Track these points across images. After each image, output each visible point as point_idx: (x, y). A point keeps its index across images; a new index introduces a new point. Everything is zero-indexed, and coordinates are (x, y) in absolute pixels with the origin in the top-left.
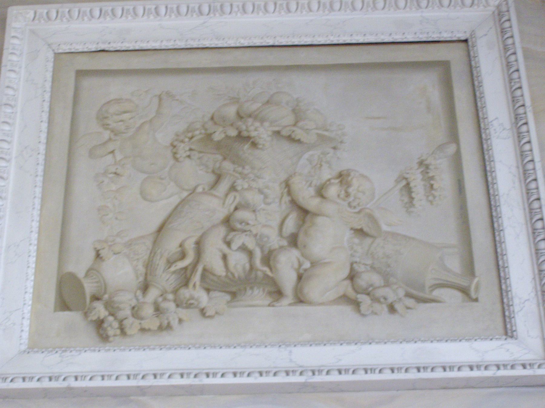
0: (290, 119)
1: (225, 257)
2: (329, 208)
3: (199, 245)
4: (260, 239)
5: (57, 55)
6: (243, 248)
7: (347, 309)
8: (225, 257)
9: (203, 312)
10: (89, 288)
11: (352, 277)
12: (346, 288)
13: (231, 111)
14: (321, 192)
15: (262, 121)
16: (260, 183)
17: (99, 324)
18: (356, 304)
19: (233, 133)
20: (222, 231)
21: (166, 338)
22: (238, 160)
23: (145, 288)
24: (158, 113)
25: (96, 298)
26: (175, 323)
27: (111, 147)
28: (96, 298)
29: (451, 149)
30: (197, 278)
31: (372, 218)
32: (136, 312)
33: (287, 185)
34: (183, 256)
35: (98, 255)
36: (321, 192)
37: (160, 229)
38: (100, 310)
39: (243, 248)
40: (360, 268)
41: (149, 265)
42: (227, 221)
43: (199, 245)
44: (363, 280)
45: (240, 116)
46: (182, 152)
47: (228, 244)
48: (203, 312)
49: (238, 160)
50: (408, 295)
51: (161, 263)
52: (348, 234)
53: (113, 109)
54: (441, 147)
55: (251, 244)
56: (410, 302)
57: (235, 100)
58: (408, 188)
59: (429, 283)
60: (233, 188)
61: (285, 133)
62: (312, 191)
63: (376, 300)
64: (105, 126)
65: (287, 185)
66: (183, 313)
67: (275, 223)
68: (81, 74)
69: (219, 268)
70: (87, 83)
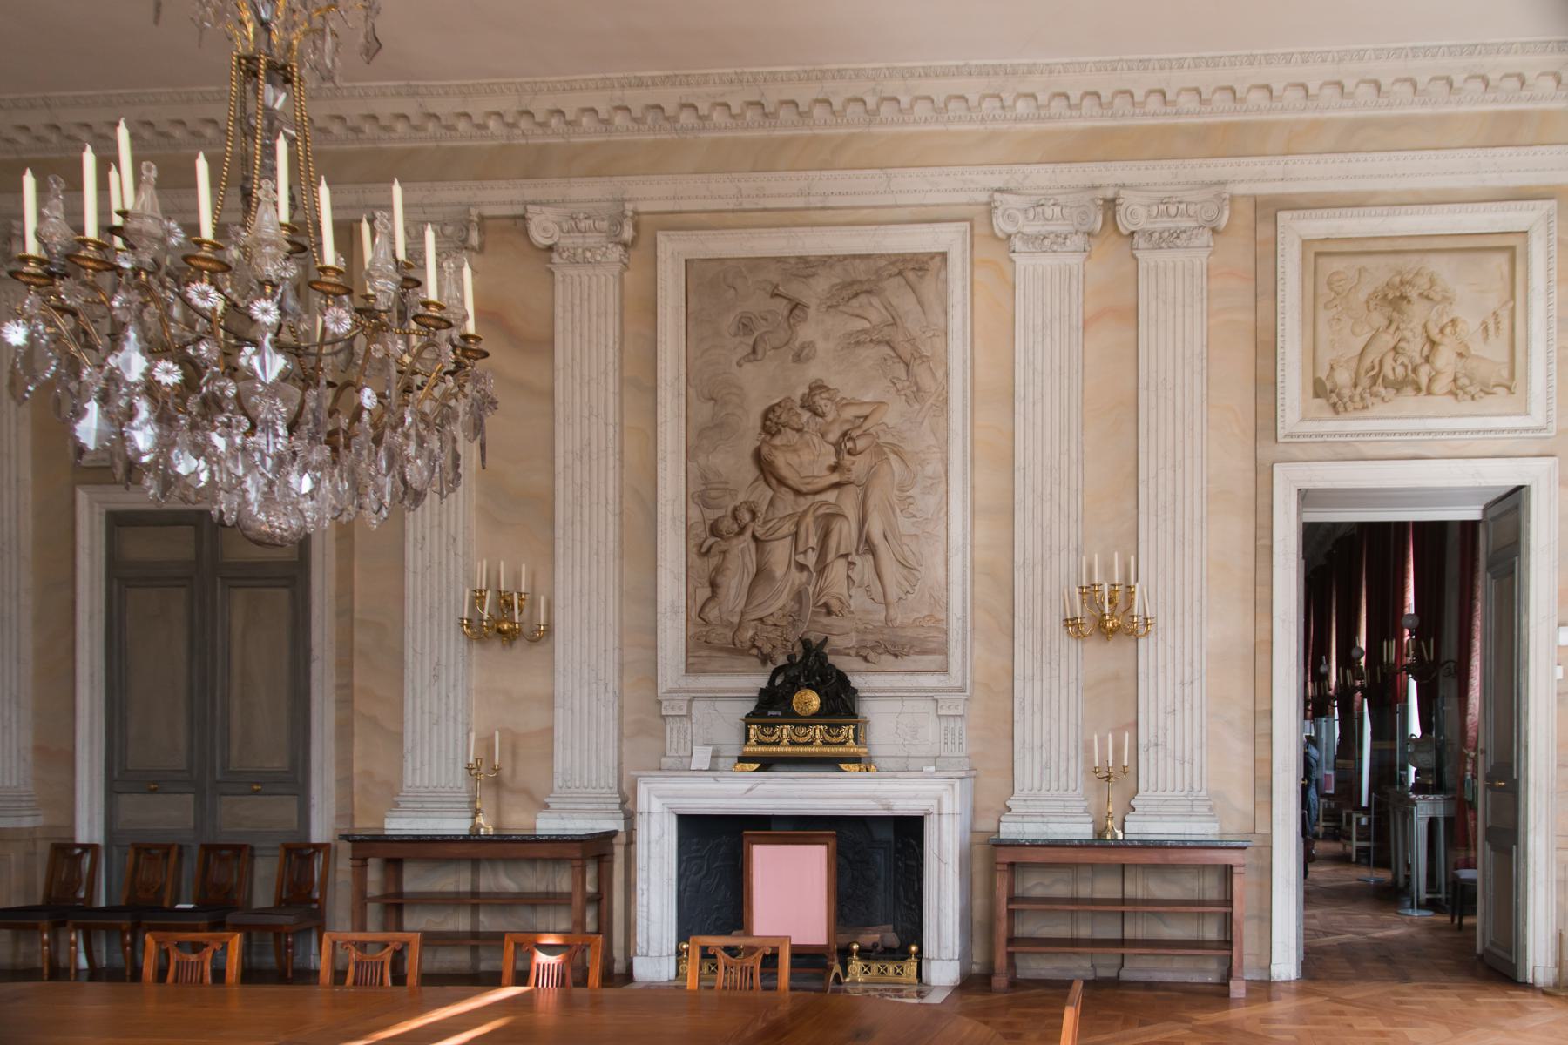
0: (1427, 286)
1: (1394, 369)
2: (1446, 340)
3: (1381, 361)
4: (1411, 359)
5: (1304, 242)
6: (1402, 364)
7: (1451, 398)
8: (1394, 369)
9: (1383, 399)
10: (1329, 386)
11: (1455, 380)
12: (1451, 386)
13: (1397, 280)
14: (1442, 331)
15: (1413, 286)
16: (1411, 326)
17: (1334, 405)
18: (1456, 395)
19: (1398, 294)
20: (1392, 354)
21: (1366, 413)
22: (1400, 312)
23: (1355, 386)
24: (1359, 280)
25: (1332, 391)
26: (1370, 405)
27: (1335, 303)
28: (1332, 391)
29: (1511, 304)
30: (1380, 380)
31: (1467, 347)
32: (1351, 399)
33: (1425, 326)
34: (1373, 368)
35: (1332, 368)
36: (1442, 331)
37: (1362, 352)
38: (1334, 398)
39: (1402, 364)
40: (1459, 375)
41: (1357, 374)
42: (1395, 348)
43: (1381, 361)
44: (1460, 383)
45: (1402, 283)
46: (1372, 306)
47: (1395, 361)
48: (1383, 399)
49: (1400, 312)
50: (1481, 390)
51: (1362, 372)
52: (1455, 355)
53: (1336, 278)
54: (1505, 303)
55: (1406, 362)
56: (1482, 394)
57: (1399, 273)
58: (1486, 329)
59: (1492, 383)
60: (1398, 328)
61: (1425, 294)
62: (1437, 330)
63: (1466, 393)
64: (1332, 289)
65: (1425, 326)
66: (1374, 400)
67: (1418, 349)
68: (1318, 254)
69: (1391, 376)
70: (1321, 260)
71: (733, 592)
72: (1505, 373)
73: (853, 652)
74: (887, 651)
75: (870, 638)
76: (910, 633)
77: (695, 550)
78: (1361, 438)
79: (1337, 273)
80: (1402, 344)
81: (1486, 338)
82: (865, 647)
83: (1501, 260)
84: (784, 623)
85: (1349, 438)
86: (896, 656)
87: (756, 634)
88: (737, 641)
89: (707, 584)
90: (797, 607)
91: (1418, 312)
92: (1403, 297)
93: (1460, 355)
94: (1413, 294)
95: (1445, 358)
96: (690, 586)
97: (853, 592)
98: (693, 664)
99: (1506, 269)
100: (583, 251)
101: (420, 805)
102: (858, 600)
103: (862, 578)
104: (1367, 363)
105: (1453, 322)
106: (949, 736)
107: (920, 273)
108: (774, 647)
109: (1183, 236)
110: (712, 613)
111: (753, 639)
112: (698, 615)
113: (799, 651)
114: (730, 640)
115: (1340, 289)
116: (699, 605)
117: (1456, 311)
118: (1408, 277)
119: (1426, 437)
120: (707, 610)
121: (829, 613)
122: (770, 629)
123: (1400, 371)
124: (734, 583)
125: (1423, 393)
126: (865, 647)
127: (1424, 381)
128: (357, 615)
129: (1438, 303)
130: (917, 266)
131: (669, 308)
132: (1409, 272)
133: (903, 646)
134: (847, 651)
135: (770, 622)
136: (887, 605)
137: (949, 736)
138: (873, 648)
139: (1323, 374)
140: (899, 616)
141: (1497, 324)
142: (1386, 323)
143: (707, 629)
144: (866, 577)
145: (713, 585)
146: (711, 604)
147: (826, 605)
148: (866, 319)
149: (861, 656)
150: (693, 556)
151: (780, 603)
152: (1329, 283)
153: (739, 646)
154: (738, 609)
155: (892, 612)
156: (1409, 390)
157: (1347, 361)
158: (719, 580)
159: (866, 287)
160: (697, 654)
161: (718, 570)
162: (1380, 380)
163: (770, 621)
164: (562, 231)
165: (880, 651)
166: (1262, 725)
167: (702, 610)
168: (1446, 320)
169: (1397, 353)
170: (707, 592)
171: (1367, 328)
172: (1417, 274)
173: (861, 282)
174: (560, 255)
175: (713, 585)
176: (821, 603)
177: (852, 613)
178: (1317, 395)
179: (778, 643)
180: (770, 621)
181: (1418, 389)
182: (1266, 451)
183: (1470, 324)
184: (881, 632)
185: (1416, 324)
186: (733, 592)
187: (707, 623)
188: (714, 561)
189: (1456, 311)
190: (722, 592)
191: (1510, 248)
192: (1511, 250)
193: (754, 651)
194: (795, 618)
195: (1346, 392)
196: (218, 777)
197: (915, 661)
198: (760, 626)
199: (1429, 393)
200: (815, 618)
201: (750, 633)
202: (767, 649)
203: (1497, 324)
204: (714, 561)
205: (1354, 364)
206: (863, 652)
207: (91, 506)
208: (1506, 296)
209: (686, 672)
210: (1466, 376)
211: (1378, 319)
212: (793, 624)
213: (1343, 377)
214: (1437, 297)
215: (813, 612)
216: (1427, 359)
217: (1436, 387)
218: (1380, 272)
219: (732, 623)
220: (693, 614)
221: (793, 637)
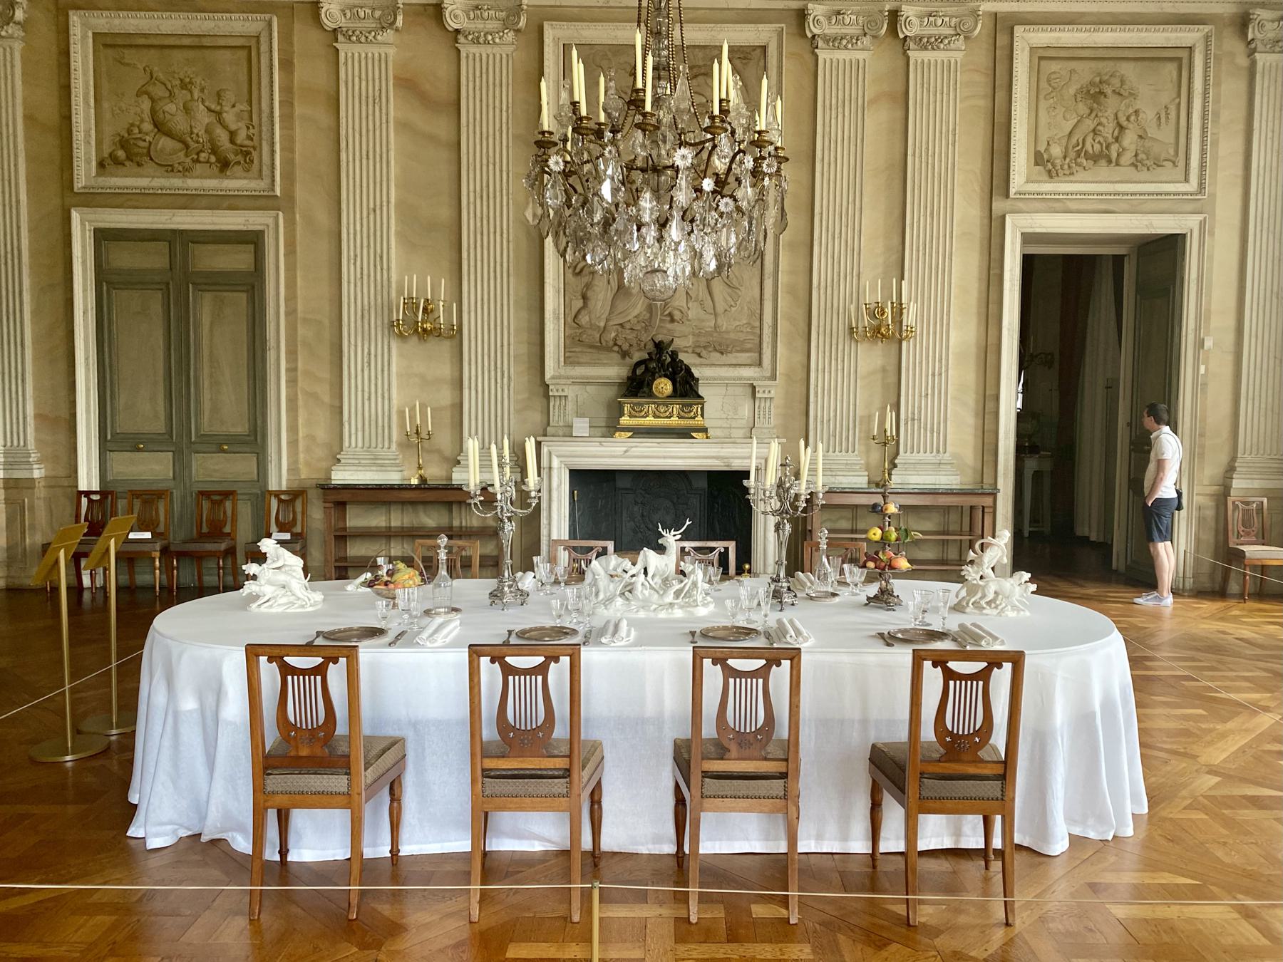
0: (1119, 85)
1: (1093, 146)
2: (1131, 126)
3: (1084, 141)
4: (1105, 139)
6: (1099, 142)
7: (1133, 168)
8: (1093, 146)
9: (1084, 168)
10: (1046, 157)
11: (1136, 155)
12: (1133, 160)
13: (1097, 79)
14: (1128, 119)
15: (1109, 85)
16: (1106, 114)
17: (1049, 171)
19: (1098, 90)
20: (1092, 134)
21: (1072, 178)
22: (1099, 104)
23: (1065, 158)
25: (1048, 161)
26: (1075, 172)
27: (1052, 95)
28: (1048, 161)
29: (1177, 101)
30: (1083, 154)
31: (1145, 130)
32: (1062, 168)
33: (1116, 115)
34: (1078, 145)
36: (1128, 119)
37: (1070, 133)
38: (1050, 166)
39: (1099, 142)
40: (1139, 152)
41: (1066, 148)
42: (1094, 131)
43: (1084, 141)
44: (1139, 158)
45: (1100, 82)
46: (1079, 99)
47: (1094, 140)
48: (1084, 168)
49: (1099, 104)
50: (1155, 164)
51: (1071, 148)
52: (1136, 137)
53: (1053, 76)
54: (1174, 100)
55: (1102, 140)
56: (1155, 166)
57: (1099, 74)
59: (1162, 158)
60: (1096, 116)
61: (1117, 91)
62: (1125, 118)
63: (1143, 165)
64: (1050, 85)
65: (1116, 115)
66: (1078, 168)
67: (1111, 132)
68: (1041, 58)
69: (1091, 152)
70: (1043, 63)
71: (600, 304)
72: (1172, 152)
73: (690, 350)
74: (716, 350)
75: (703, 340)
76: (732, 336)
77: (571, 270)
78: (1070, 197)
79: (1054, 73)
80: (1100, 128)
81: (1159, 125)
82: (699, 346)
83: (1171, 68)
84: (639, 328)
85: (1061, 197)
86: (722, 353)
87: (617, 335)
88: (603, 341)
89: (580, 297)
90: (648, 315)
91: (1112, 103)
92: (1101, 92)
93: (1140, 137)
94: (1108, 90)
95: (1129, 139)
96: (566, 298)
97: (690, 305)
98: (569, 357)
99: (1175, 74)
100: (485, 36)
101: (357, 462)
102: (694, 312)
103: (698, 295)
104: (1074, 141)
105: (1136, 112)
106: (762, 413)
107: (744, 61)
108: (631, 345)
109: (946, 41)
110: (584, 319)
111: (615, 339)
112: (573, 320)
113: (651, 347)
114: (598, 339)
115: (1056, 85)
116: (573, 314)
117: (1138, 105)
118: (1105, 78)
119: (1117, 197)
120: (580, 317)
121: (672, 320)
122: (628, 332)
123: (1097, 147)
124: (601, 296)
125: (1114, 164)
126: (699, 346)
127: (1114, 155)
128: (300, 315)
129: (1126, 98)
130: (742, 56)
131: (551, 82)
132: (1106, 74)
133: (728, 346)
134: (685, 349)
135: (628, 327)
136: (716, 315)
137: (762, 413)
138: (705, 347)
139: (1042, 148)
140: (724, 324)
141: (1167, 114)
142: (1088, 111)
143: (580, 331)
144: (701, 294)
145: (585, 297)
146: (583, 312)
147: (670, 315)
148: (703, 95)
149: (696, 353)
150: (569, 275)
151: (636, 312)
152: (1049, 81)
153: (604, 344)
154: (604, 316)
155: (719, 321)
156: (1103, 162)
157: (1059, 139)
158: (589, 294)
159: (703, 71)
160: (573, 350)
161: (588, 286)
162: (1083, 154)
163: (628, 326)
164: (469, 19)
165: (710, 349)
166: (990, 405)
167: (575, 317)
168: (1131, 111)
169: (1096, 134)
170: (580, 303)
171: (1075, 115)
172: (1111, 76)
173: (699, 67)
174: (466, 37)
175: (585, 297)
176: (667, 313)
177: (689, 320)
178: (1037, 164)
179: (634, 342)
180: (628, 326)
181: (1110, 162)
182: (998, 205)
183: (1148, 115)
184: (712, 336)
185: (1110, 113)
186: (600, 304)
187: (580, 326)
188: (585, 279)
189: (1138, 105)
190: (591, 304)
191: (1180, 59)
192: (1179, 60)
193: (616, 348)
194: (648, 325)
195: (1058, 162)
196: (193, 439)
197: (736, 357)
198: (620, 329)
199: (1117, 164)
200: (662, 325)
201: (613, 335)
202: (625, 347)
203: (1167, 114)
204: (585, 279)
205: (1064, 142)
206: (698, 350)
207: (82, 224)
208: (1174, 95)
209: (565, 363)
210: (1143, 152)
211: (1083, 108)
212: (646, 329)
213: (1056, 151)
214: (1125, 94)
215: (661, 320)
216: (1117, 140)
217: (1123, 160)
218: (1085, 72)
219: (599, 327)
220: (570, 320)
221: (646, 338)
